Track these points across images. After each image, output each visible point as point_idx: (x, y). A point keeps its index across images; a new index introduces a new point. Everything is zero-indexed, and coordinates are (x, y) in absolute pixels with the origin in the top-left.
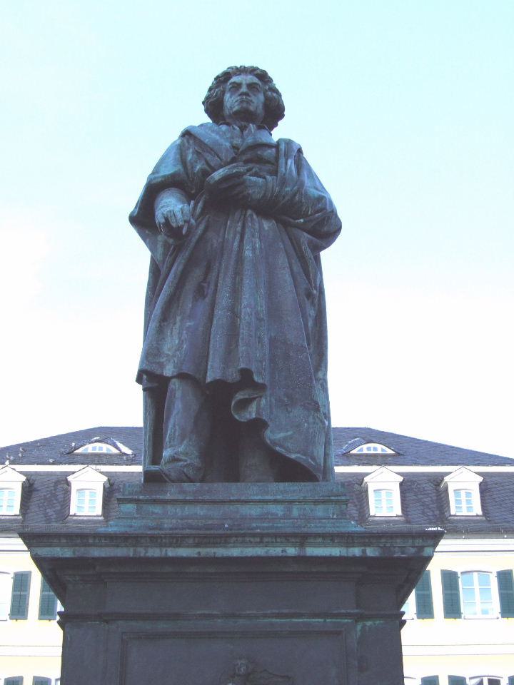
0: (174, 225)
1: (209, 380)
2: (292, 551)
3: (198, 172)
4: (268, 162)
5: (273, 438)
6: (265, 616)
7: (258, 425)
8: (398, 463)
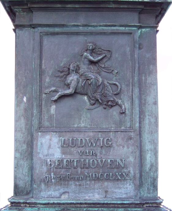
6: (100, 26)
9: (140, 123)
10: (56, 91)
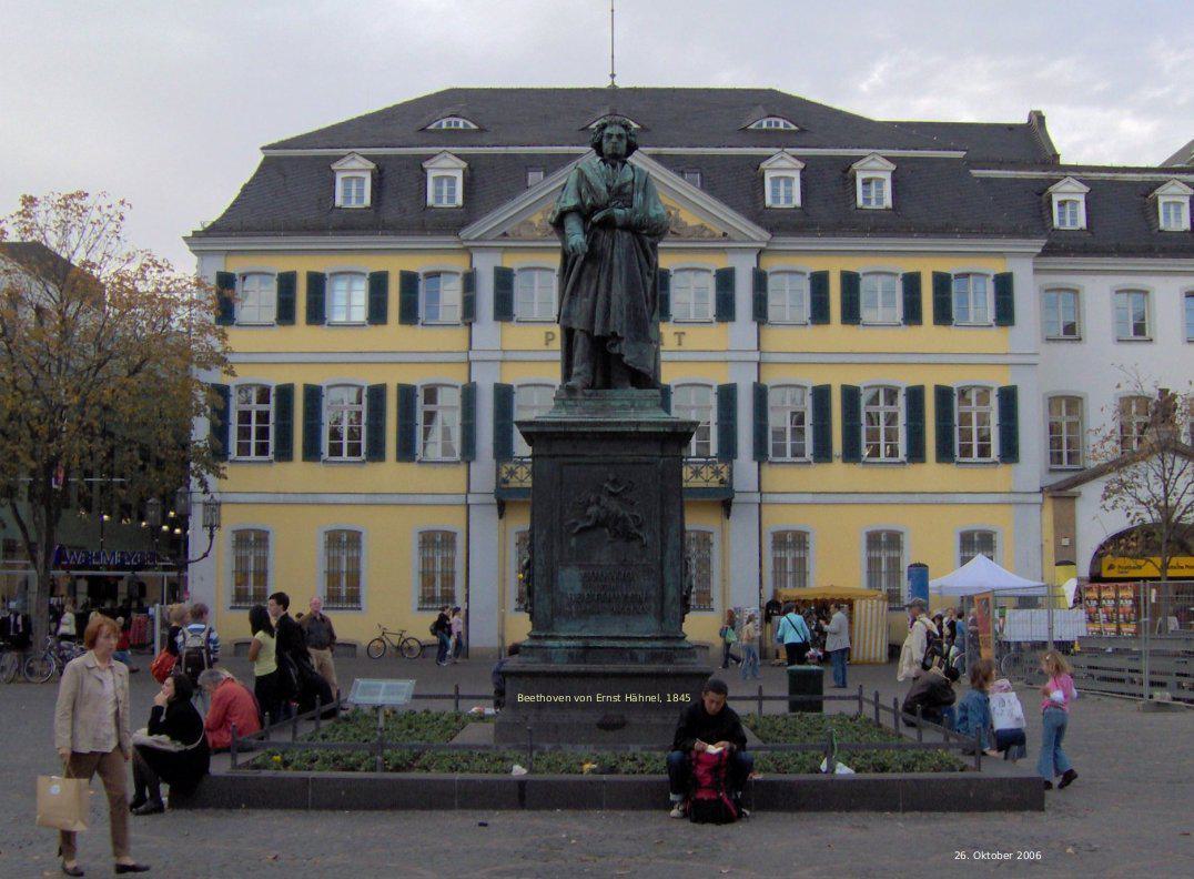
1: (595, 334)
2: (633, 429)
4: (628, 193)
7: (620, 356)
8: (803, 144)
9: (662, 555)
10: (576, 524)
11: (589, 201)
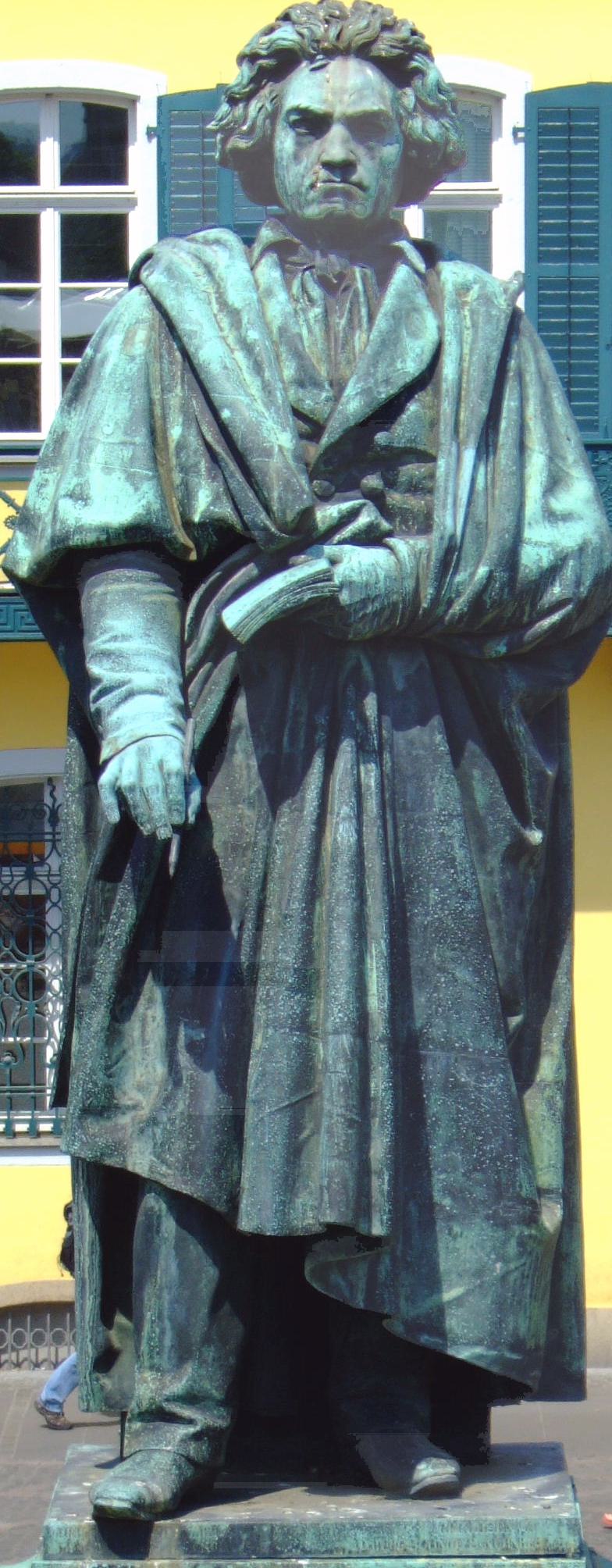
0: (146, 830)
3: (202, 525)
5: (413, 1313)
11: (204, 501)
